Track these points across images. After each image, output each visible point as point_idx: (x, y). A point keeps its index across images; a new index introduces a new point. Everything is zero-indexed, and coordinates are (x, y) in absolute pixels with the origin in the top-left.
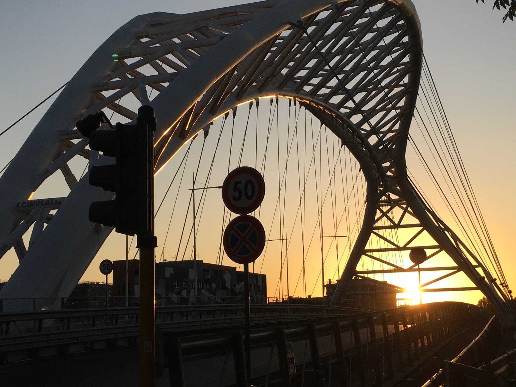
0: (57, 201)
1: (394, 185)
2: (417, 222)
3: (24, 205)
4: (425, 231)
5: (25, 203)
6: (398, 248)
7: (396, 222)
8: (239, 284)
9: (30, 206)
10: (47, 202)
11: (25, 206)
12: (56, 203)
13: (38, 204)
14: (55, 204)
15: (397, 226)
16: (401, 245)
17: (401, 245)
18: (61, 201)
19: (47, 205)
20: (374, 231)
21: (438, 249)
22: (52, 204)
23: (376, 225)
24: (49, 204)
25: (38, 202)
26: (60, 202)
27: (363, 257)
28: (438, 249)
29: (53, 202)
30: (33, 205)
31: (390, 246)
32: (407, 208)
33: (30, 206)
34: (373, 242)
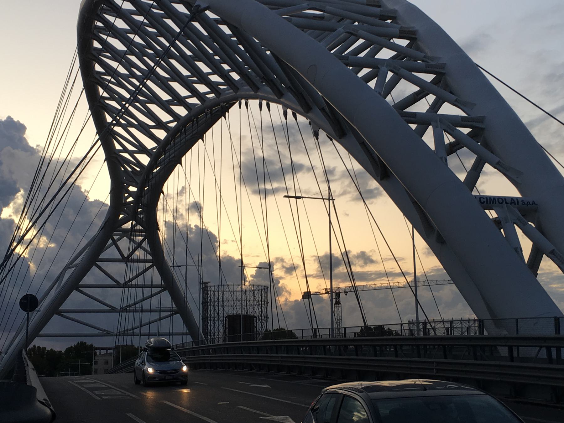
0: (524, 201)
1: (141, 213)
2: (149, 257)
3: (482, 201)
5: (484, 199)
6: (118, 285)
7: (126, 255)
9: (490, 203)
10: (512, 201)
11: (484, 202)
12: (523, 203)
13: (501, 201)
14: (522, 204)
15: (126, 260)
18: (529, 203)
19: (512, 204)
21: (160, 289)
22: (518, 204)
23: (101, 256)
24: (515, 204)
25: (501, 201)
26: (528, 203)
29: (520, 203)
30: (494, 203)
31: (134, 282)
32: (142, 241)
33: (490, 203)
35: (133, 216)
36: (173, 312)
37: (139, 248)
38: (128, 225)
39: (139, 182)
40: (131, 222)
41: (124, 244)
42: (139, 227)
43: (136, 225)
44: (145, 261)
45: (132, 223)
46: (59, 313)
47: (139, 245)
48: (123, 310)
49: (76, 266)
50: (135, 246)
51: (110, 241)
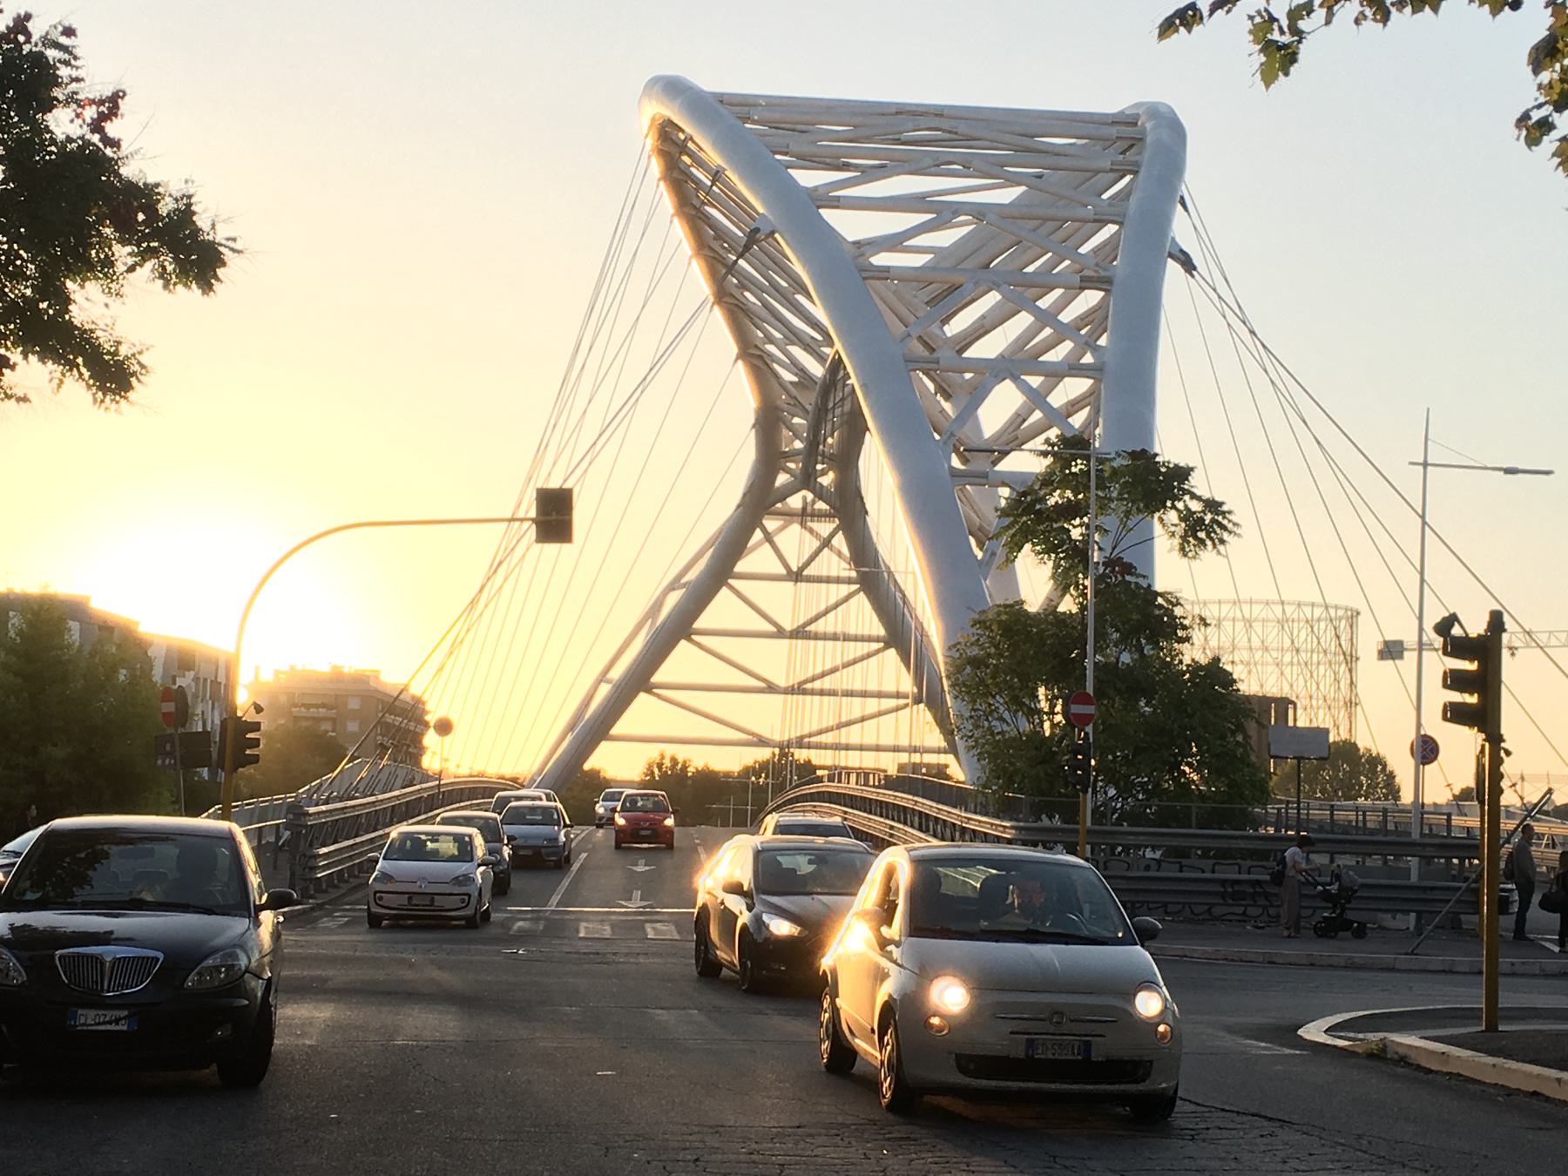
4: (862, 593)
6: (780, 633)
8: (184, 676)
15: (797, 576)
16: (788, 627)
17: (788, 627)
20: (730, 581)
23: (741, 567)
27: (683, 643)
28: (882, 645)
32: (832, 535)
34: (722, 610)
35: (807, 480)
36: (918, 700)
37: (826, 550)
38: (795, 502)
39: (809, 408)
40: (804, 492)
41: (794, 541)
42: (821, 505)
43: (814, 502)
44: (838, 580)
45: (804, 498)
46: (650, 690)
47: (826, 543)
48: (798, 690)
49: (684, 585)
50: (816, 544)
51: (758, 535)
